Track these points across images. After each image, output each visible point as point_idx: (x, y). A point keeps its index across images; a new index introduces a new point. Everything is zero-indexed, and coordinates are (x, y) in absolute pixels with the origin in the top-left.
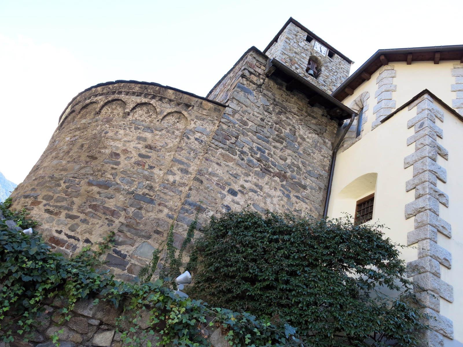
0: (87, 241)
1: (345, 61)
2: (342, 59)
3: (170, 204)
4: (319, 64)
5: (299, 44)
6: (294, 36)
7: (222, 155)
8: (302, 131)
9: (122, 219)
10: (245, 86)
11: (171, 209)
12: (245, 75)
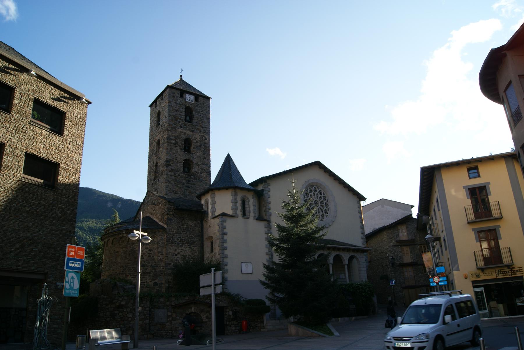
8: (190, 223)
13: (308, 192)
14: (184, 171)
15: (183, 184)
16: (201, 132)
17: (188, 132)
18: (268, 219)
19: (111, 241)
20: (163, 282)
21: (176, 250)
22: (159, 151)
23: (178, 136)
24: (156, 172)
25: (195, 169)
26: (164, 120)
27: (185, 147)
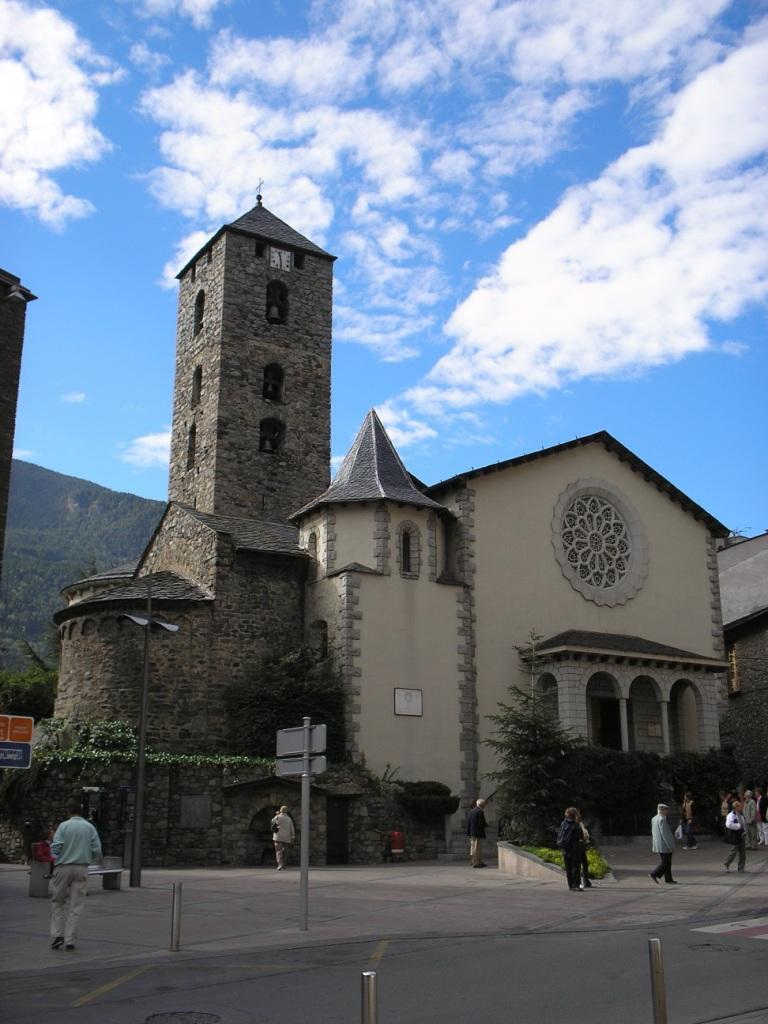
0: (163, 728)
1: (322, 261)
3: (201, 689)
5: (247, 273)
6: (237, 259)
7: (222, 641)
8: (272, 586)
9: (178, 709)
11: (202, 692)
13: (575, 513)
14: (262, 449)
15: (259, 483)
16: (306, 348)
17: (274, 348)
18: (467, 582)
19: (80, 625)
20: (203, 730)
21: (235, 652)
22: (199, 396)
23: (247, 359)
24: (192, 450)
25: (290, 444)
26: (214, 316)
27: (266, 385)
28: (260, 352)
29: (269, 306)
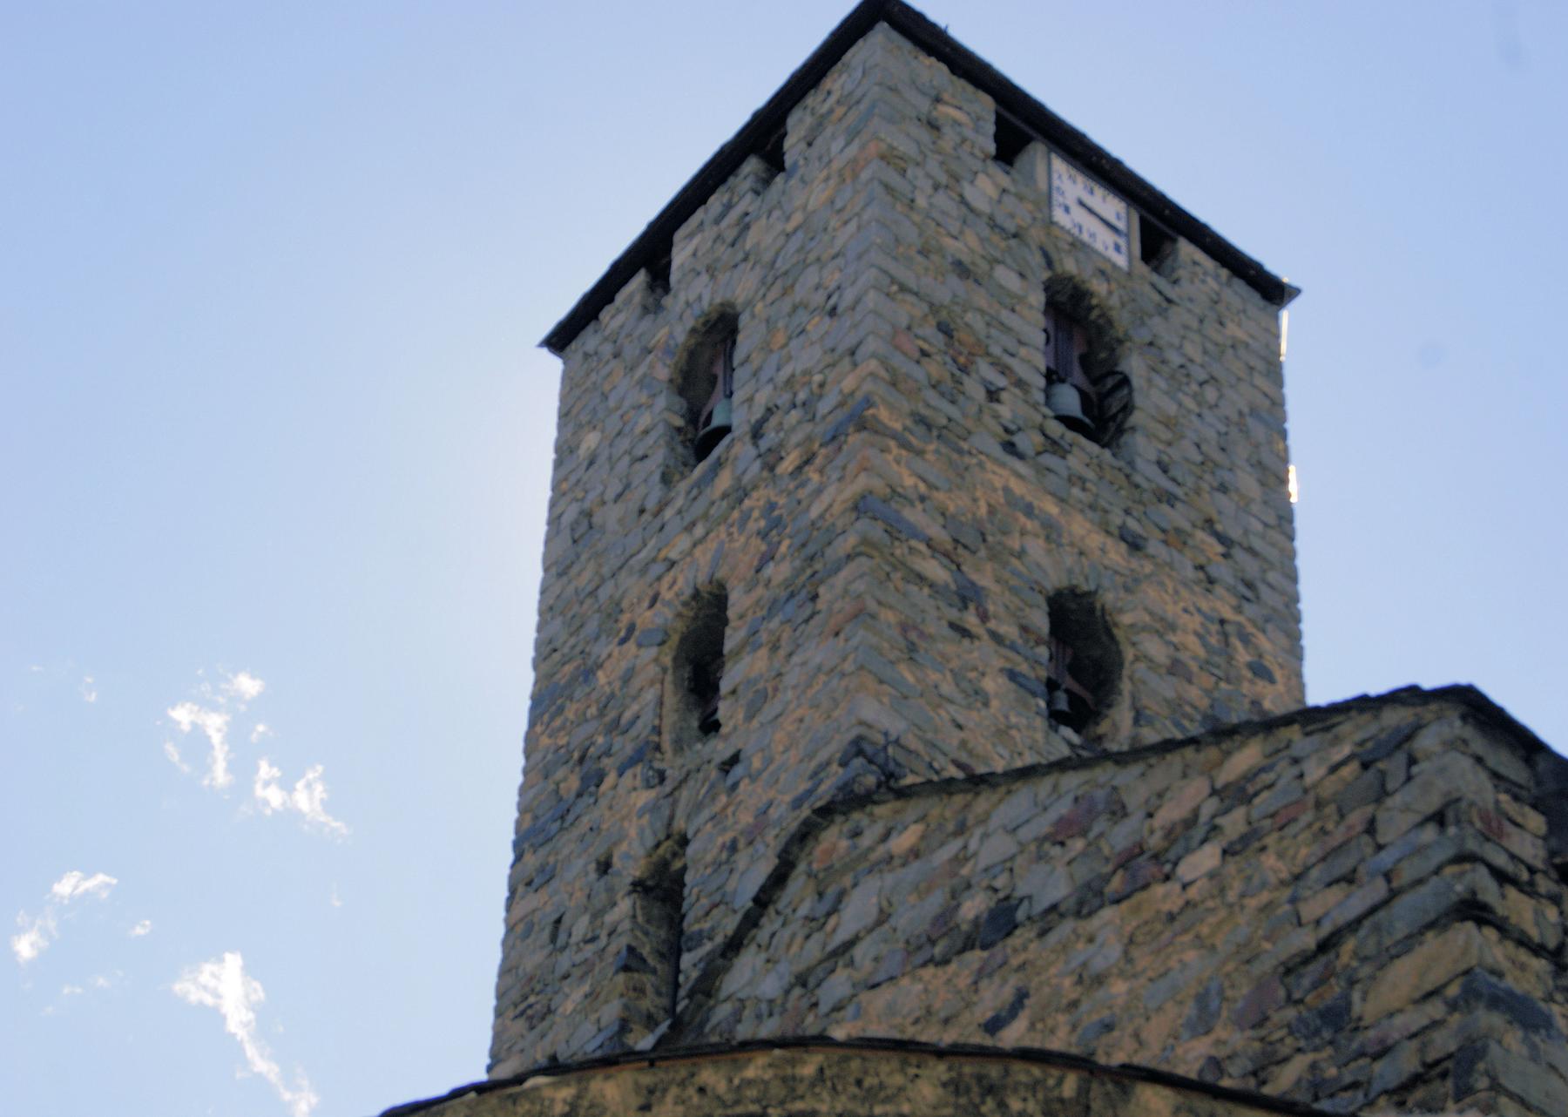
1: (1239, 285)
2: (1224, 273)
4: (1101, 331)
10: (1509, 982)
12: (1485, 907)
17: (1079, 527)
28: (1030, 525)
29: (1053, 377)
